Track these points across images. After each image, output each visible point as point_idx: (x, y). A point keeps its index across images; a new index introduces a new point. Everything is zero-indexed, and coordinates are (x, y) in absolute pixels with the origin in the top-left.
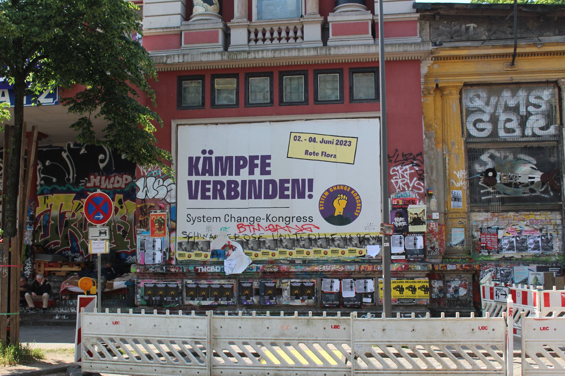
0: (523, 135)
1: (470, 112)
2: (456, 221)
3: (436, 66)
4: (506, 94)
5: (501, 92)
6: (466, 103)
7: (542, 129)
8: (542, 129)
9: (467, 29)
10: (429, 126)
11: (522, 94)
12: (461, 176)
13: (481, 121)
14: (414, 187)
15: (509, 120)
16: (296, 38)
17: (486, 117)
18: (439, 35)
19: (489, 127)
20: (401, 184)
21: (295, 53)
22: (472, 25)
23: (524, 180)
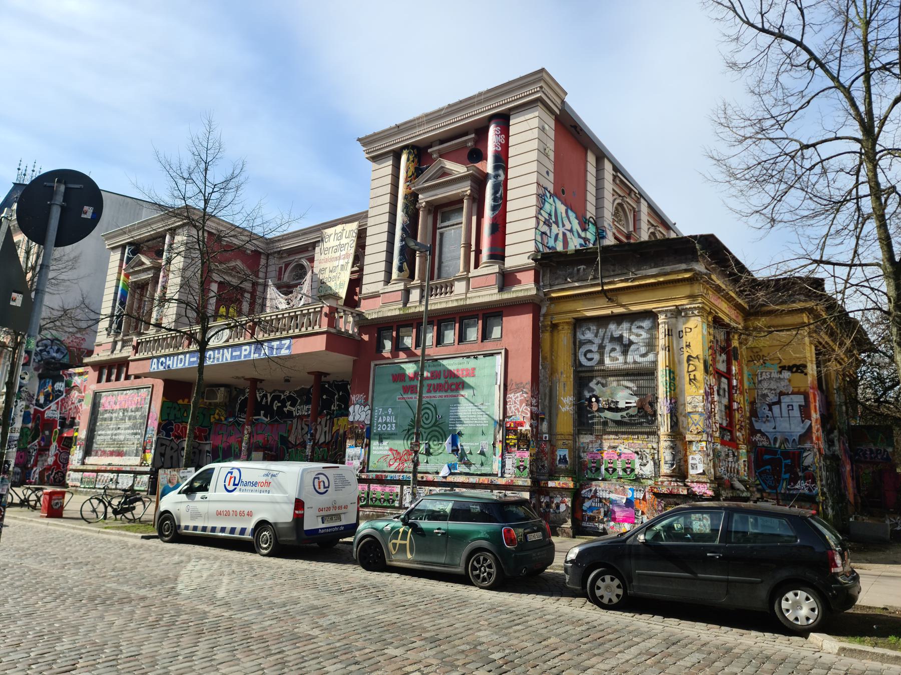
0: (626, 363)
1: (582, 343)
2: (560, 442)
3: (553, 306)
4: (612, 327)
5: (608, 324)
6: (580, 337)
7: (643, 355)
8: (643, 355)
9: (578, 270)
10: (544, 358)
11: (625, 325)
12: (568, 402)
13: (590, 351)
14: (522, 412)
15: (613, 350)
16: (451, 292)
17: (594, 348)
18: (556, 279)
19: (596, 357)
20: (513, 409)
21: (443, 306)
22: (582, 267)
23: (622, 405)
